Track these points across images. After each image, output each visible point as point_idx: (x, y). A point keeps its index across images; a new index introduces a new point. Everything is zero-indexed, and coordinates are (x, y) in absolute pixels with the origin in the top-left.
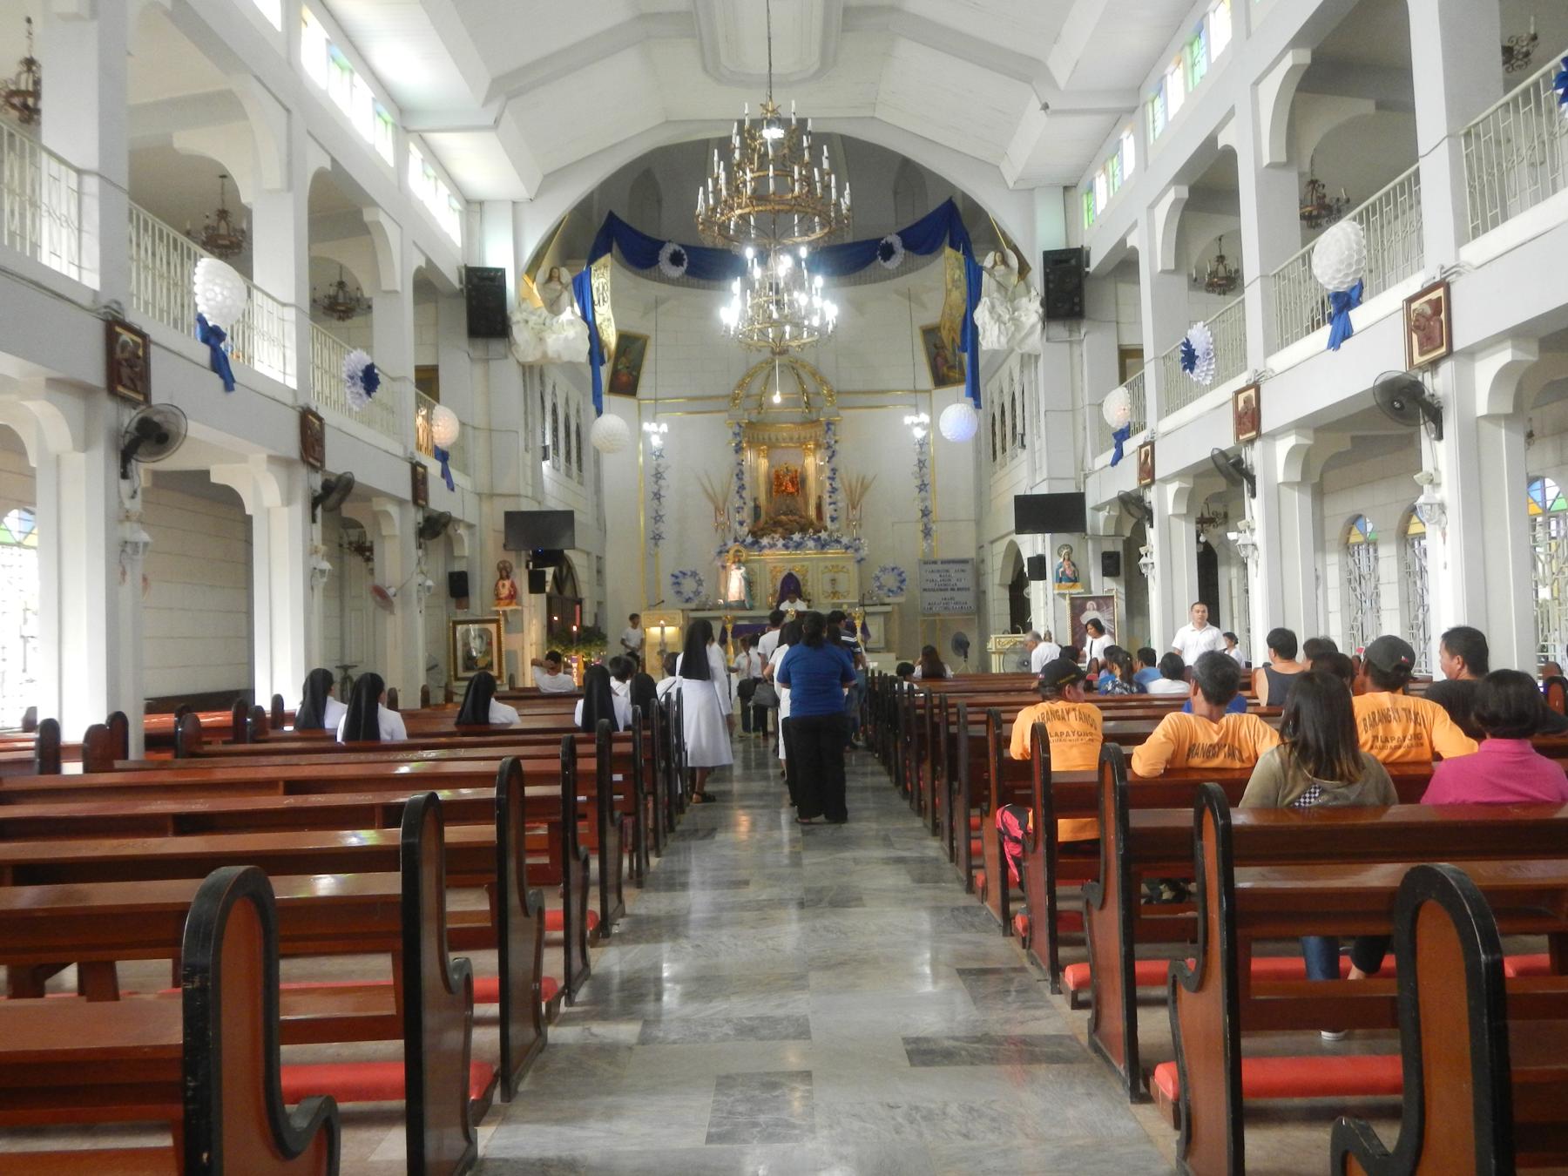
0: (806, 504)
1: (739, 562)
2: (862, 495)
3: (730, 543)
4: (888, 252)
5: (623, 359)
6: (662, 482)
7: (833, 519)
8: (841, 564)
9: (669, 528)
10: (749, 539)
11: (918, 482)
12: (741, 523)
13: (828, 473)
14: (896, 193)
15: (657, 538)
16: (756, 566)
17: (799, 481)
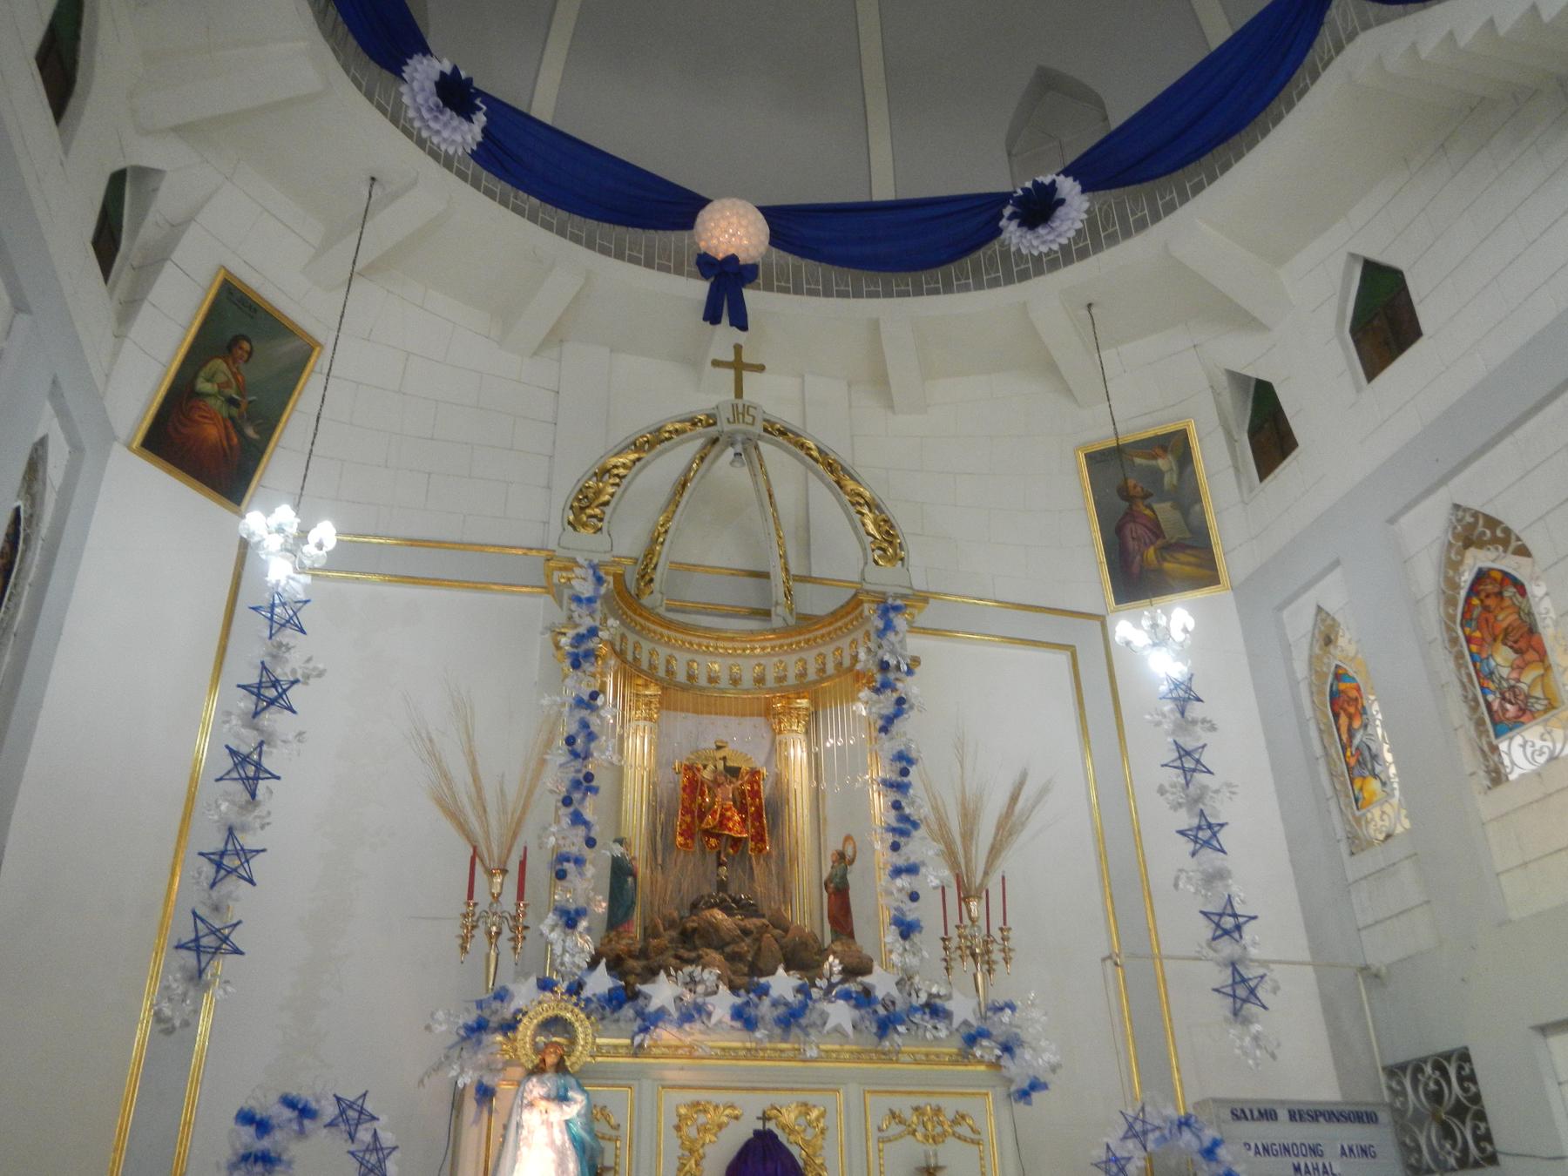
0: (785, 889)
1: (556, 1067)
2: (995, 851)
3: (524, 994)
4: (1038, 207)
5: (219, 365)
6: (274, 719)
7: (907, 929)
8: (950, 1106)
9: (262, 910)
10: (600, 982)
11: (1186, 820)
12: (570, 920)
13: (880, 770)
14: (1009, 154)
15: (207, 944)
16: (617, 1099)
17: (761, 810)
